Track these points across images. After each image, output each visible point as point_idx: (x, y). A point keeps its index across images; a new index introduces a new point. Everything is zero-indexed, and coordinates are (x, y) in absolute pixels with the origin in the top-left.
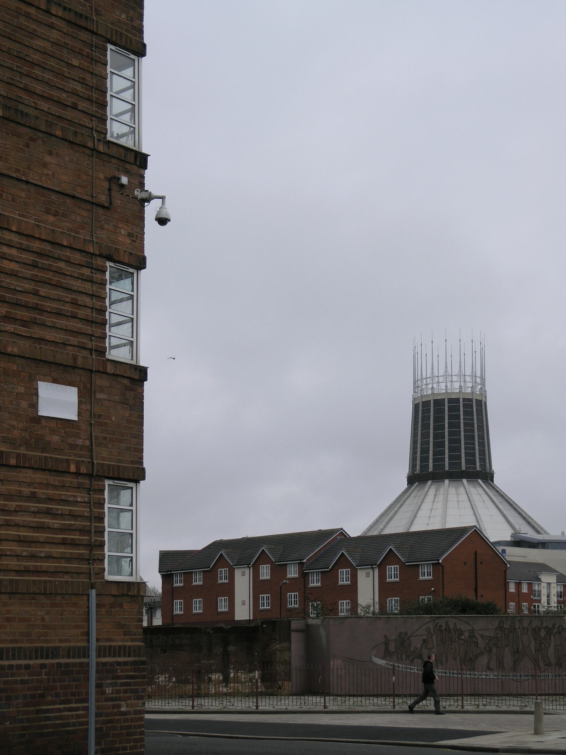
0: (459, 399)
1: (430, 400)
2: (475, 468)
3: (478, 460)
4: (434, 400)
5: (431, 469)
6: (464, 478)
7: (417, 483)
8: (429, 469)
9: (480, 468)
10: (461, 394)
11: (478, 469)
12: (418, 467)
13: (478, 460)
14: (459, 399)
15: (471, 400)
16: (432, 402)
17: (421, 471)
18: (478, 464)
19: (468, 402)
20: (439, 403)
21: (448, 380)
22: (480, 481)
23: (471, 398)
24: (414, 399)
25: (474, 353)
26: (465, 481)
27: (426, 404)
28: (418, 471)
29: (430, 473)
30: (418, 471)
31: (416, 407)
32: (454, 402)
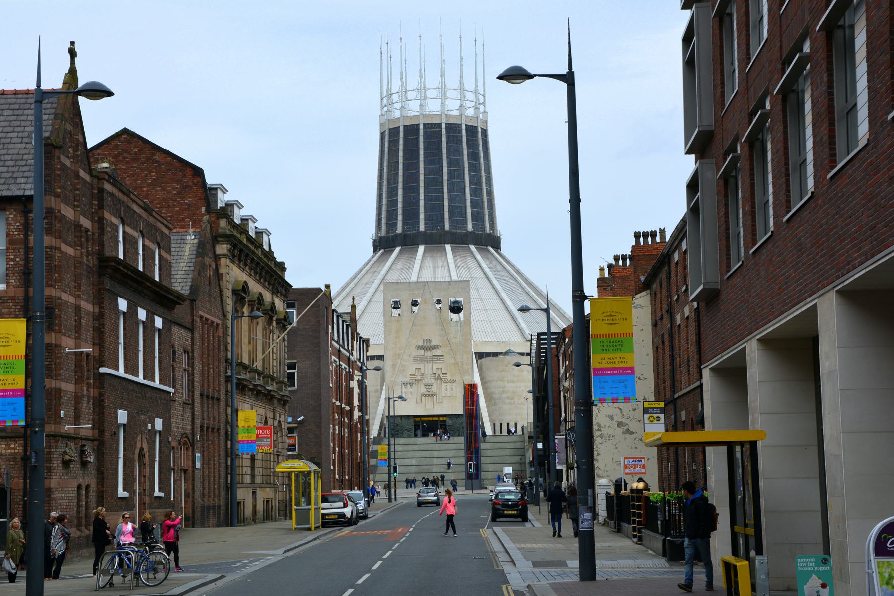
0: (441, 124)
4: (404, 126)
5: (399, 230)
6: (448, 243)
7: (382, 251)
8: (396, 229)
9: (473, 228)
11: (470, 228)
12: (384, 227)
16: (402, 129)
17: (388, 231)
19: (453, 129)
20: (412, 130)
22: (472, 247)
23: (460, 123)
24: (381, 124)
25: (404, 62)
26: (448, 248)
27: (394, 132)
28: (383, 233)
29: (397, 235)
30: (383, 233)
31: (382, 135)
32: (432, 129)
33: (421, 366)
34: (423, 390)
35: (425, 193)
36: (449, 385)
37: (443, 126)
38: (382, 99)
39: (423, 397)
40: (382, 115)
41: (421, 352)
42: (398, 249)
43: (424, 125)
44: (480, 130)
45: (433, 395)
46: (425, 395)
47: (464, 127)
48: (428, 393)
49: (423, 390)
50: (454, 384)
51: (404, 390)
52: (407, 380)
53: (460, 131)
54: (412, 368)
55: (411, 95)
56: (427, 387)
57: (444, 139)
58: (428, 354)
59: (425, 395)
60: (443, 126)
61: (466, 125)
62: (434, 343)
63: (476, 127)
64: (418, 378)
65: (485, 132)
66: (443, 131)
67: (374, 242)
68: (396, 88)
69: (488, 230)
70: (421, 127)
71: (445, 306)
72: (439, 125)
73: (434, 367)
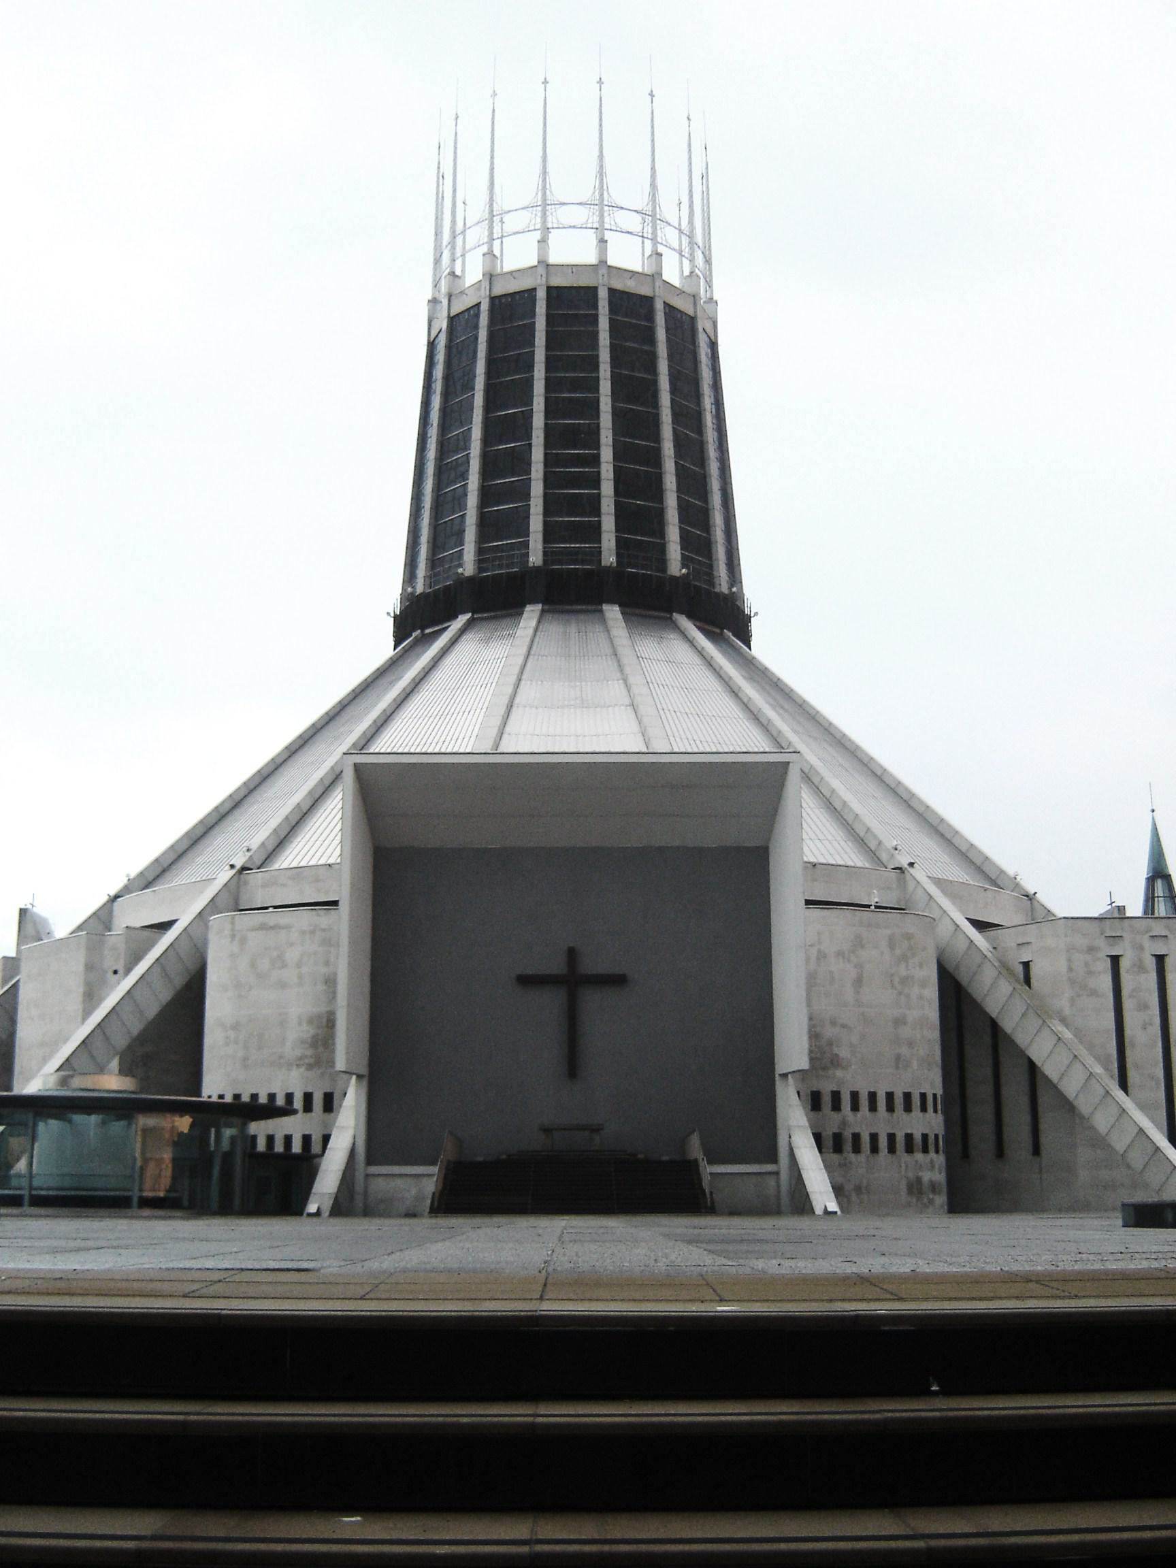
0: (596, 288)
1: (479, 305)
2: (662, 562)
3: (670, 482)
5: (468, 567)
9: (684, 566)
10: (603, 271)
13: (670, 482)
14: (596, 288)
15: (648, 301)
16: (485, 307)
18: (674, 552)
21: (549, 219)
26: (613, 612)
28: (420, 588)
31: (431, 346)
35: (546, 465)
37: (603, 294)
38: (437, 261)
40: (434, 302)
42: (463, 619)
43: (549, 289)
44: (700, 329)
47: (659, 306)
53: (650, 316)
55: (513, 222)
60: (603, 294)
61: (664, 302)
63: (693, 319)
65: (713, 345)
67: (398, 620)
68: (476, 209)
69: (723, 585)
70: (541, 294)
72: (593, 290)
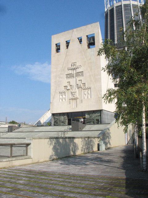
33: (70, 80)
34: (71, 97)
36: (86, 90)
39: (71, 101)
41: (70, 72)
45: (76, 99)
46: (72, 99)
48: (73, 97)
49: (71, 97)
50: (90, 90)
51: (61, 97)
52: (63, 89)
54: (65, 81)
56: (73, 94)
57: (123, 9)
58: (74, 72)
59: (72, 99)
62: (78, 64)
64: (69, 88)
66: (123, 7)
71: (85, 42)
73: (77, 80)
